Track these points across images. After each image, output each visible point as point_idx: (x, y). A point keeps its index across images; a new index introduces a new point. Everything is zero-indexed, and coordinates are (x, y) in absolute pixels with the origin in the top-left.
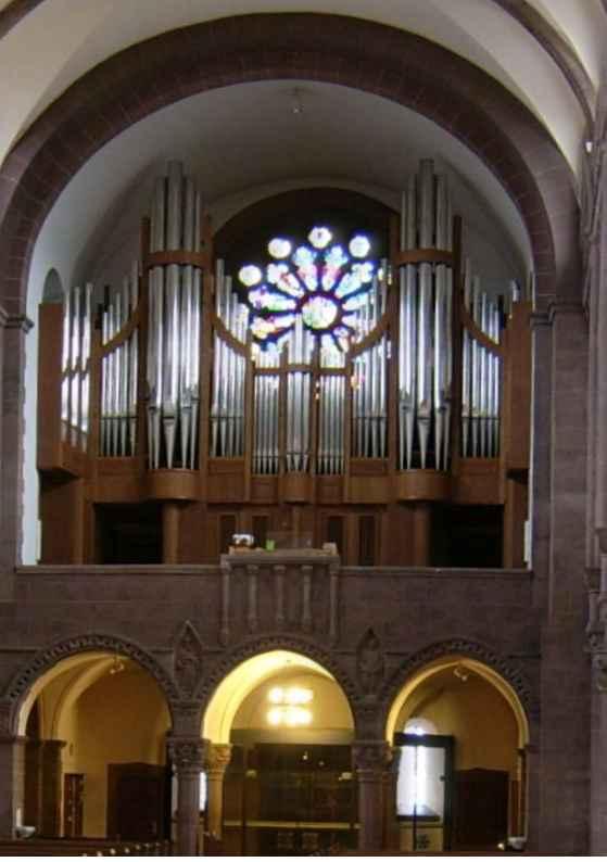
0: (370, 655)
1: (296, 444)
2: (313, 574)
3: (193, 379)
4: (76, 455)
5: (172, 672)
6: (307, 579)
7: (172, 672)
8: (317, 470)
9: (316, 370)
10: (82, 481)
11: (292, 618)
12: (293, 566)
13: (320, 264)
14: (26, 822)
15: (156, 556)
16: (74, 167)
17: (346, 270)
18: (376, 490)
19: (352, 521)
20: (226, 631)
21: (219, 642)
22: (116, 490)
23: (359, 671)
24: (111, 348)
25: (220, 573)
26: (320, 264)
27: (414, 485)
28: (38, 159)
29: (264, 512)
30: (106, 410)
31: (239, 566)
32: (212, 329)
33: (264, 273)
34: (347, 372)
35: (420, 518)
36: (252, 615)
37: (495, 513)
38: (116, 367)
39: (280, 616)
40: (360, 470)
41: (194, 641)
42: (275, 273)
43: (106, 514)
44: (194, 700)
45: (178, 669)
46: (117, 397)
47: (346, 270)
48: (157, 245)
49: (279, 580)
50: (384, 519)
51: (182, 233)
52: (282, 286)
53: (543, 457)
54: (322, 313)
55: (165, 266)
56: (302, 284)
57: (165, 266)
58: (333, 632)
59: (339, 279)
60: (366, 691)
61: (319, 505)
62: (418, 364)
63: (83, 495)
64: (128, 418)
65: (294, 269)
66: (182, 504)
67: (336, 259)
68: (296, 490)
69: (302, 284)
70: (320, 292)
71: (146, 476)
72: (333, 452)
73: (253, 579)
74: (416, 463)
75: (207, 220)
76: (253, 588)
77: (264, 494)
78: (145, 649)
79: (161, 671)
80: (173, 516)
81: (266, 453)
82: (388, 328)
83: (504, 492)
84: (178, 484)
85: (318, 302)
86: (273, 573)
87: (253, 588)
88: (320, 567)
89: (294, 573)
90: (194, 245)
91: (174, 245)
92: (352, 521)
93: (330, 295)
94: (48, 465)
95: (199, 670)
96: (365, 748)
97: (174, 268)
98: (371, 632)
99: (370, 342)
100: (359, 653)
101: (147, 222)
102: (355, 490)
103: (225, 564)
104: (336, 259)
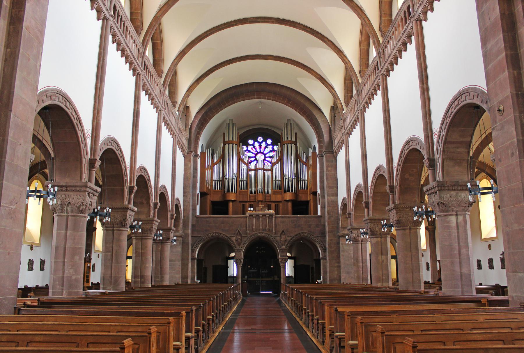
0: (283, 236)
1: (260, 187)
2: (269, 217)
3: (235, 171)
4: (207, 188)
5: (235, 241)
6: (267, 218)
7: (235, 241)
8: (265, 193)
9: (264, 170)
10: (209, 196)
11: (264, 228)
12: (264, 215)
13: (260, 146)
14: (197, 280)
15: (226, 212)
16: (210, 118)
17: (266, 147)
18: (279, 198)
19: (273, 205)
20: (248, 231)
21: (246, 234)
22: (217, 198)
23: (281, 241)
24: (215, 164)
25: (246, 217)
26: (260, 146)
27: (289, 196)
28: (203, 116)
29: (252, 203)
30: (214, 178)
31: (251, 216)
32: (240, 160)
33: (247, 148)
34: (271, 170)
35: (290, 204)
36: (254, 227)
37: (307, 203)
38: (217, 169)
39: (261, 227)
40: (275, 193)
41: (240, 233)
42: (250, 148)
43: (214, 203)
44: (240, 248)
45: (236, 240)
46: (217, 176)
47: (266, 147)
48: (227, 139)
49: (261, 219)
50: (281, 205)
51: (233, 136)
52: (251, 151)
53: (322, 188)
54: (260, 157)
55: (229, 144)
56: (256, 151)
57: (229, 144)
58: (274, 231)
59: (265, 149)
60: (282, 245)
61: (265, 201)
62: (289, 169)
63: (209, 199)
64: (220, 181)
65: (254, 147)
66: (233, 201)
67: (264, 145)
68: (260, 198)
69: (256, 151)
70: (260, 152)
71: (224, 194)
72: (268, 188)
73: (254, 219)
74: (289, 191)
75: (238, 133)
76: (254, 221)
77: (252, 199)
78: (228, 236)
79: (232, 241)
80: (231, 204)
81: (253, 189)
82: (281, 160)
83: (310, 198)
84: (232, 196)
85: (260, 155)
86: (266, 217)
87: (254, 221)
88: (271, 215)
89: (264, 217)
90: (235, 139)
91: (231, 139)
92: (273, 205)
93: (262, 153)
94: (202, 191)
95: (241, 240)
96: (282, 259)
97: (231, 145)
98: (283, 231)
99: (277, 162)
100: (280, 236)
101: (224, 134)
102: (274, 198)
103: (247, 215)
104: (264, 145)
